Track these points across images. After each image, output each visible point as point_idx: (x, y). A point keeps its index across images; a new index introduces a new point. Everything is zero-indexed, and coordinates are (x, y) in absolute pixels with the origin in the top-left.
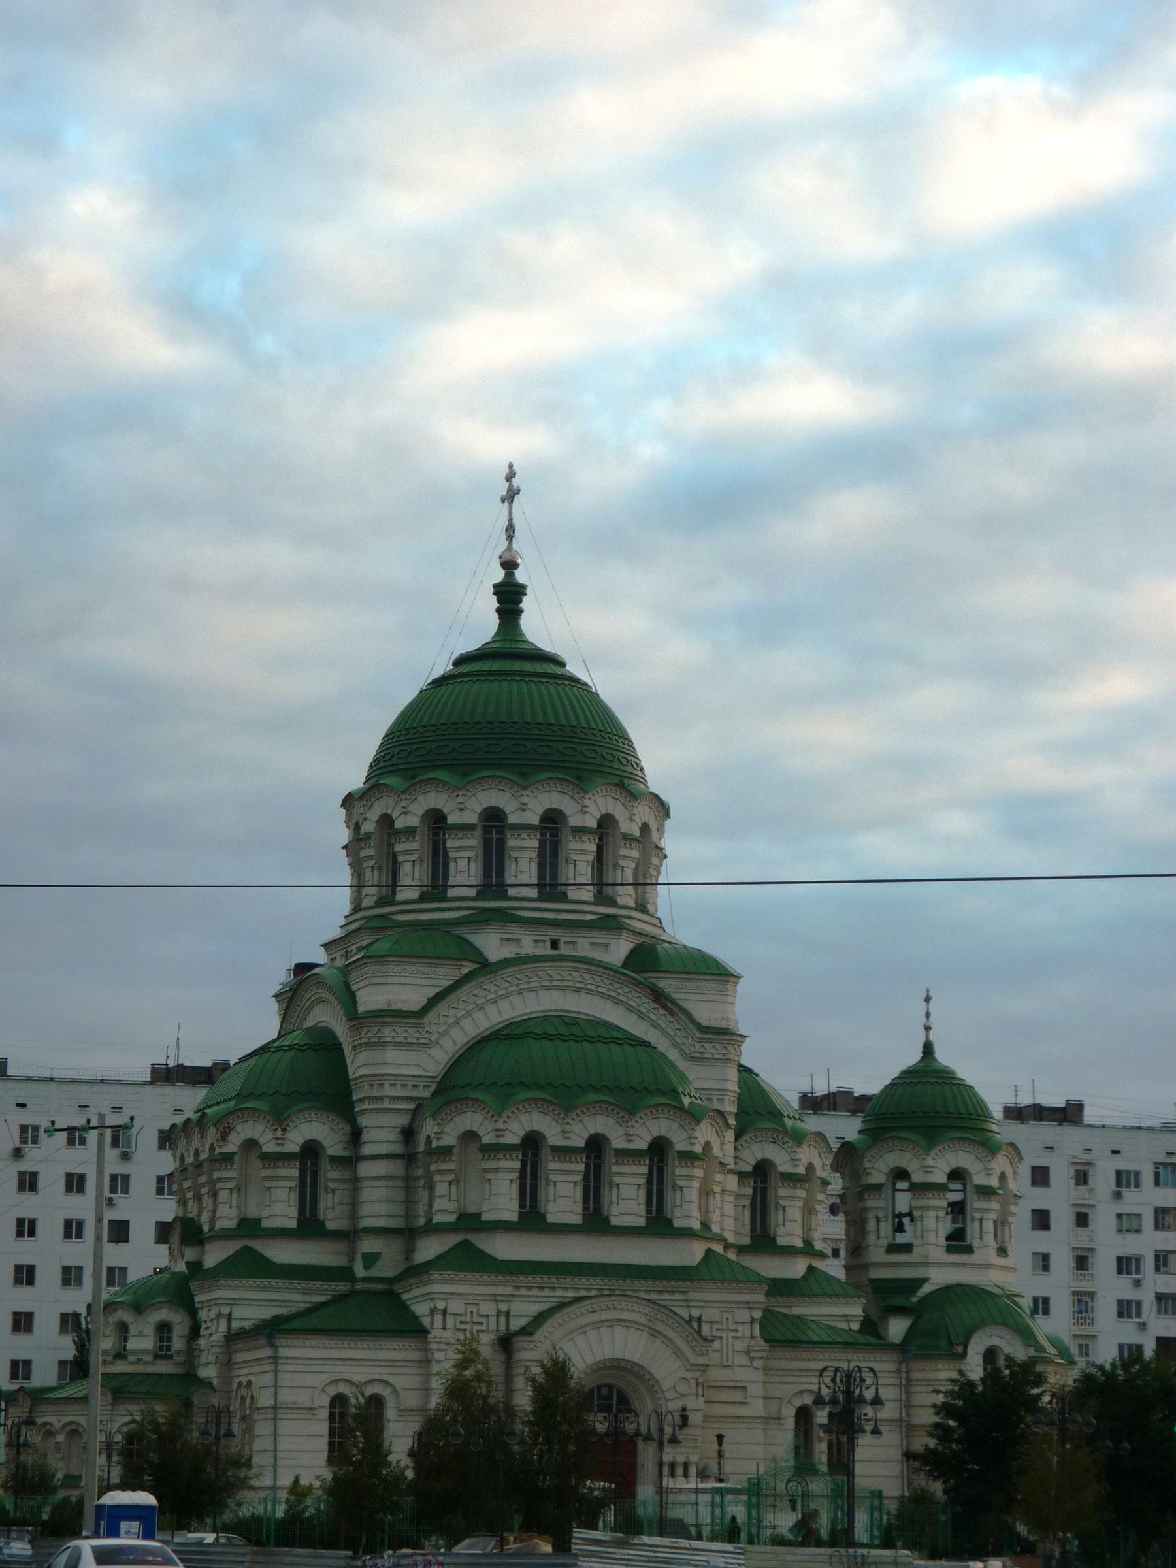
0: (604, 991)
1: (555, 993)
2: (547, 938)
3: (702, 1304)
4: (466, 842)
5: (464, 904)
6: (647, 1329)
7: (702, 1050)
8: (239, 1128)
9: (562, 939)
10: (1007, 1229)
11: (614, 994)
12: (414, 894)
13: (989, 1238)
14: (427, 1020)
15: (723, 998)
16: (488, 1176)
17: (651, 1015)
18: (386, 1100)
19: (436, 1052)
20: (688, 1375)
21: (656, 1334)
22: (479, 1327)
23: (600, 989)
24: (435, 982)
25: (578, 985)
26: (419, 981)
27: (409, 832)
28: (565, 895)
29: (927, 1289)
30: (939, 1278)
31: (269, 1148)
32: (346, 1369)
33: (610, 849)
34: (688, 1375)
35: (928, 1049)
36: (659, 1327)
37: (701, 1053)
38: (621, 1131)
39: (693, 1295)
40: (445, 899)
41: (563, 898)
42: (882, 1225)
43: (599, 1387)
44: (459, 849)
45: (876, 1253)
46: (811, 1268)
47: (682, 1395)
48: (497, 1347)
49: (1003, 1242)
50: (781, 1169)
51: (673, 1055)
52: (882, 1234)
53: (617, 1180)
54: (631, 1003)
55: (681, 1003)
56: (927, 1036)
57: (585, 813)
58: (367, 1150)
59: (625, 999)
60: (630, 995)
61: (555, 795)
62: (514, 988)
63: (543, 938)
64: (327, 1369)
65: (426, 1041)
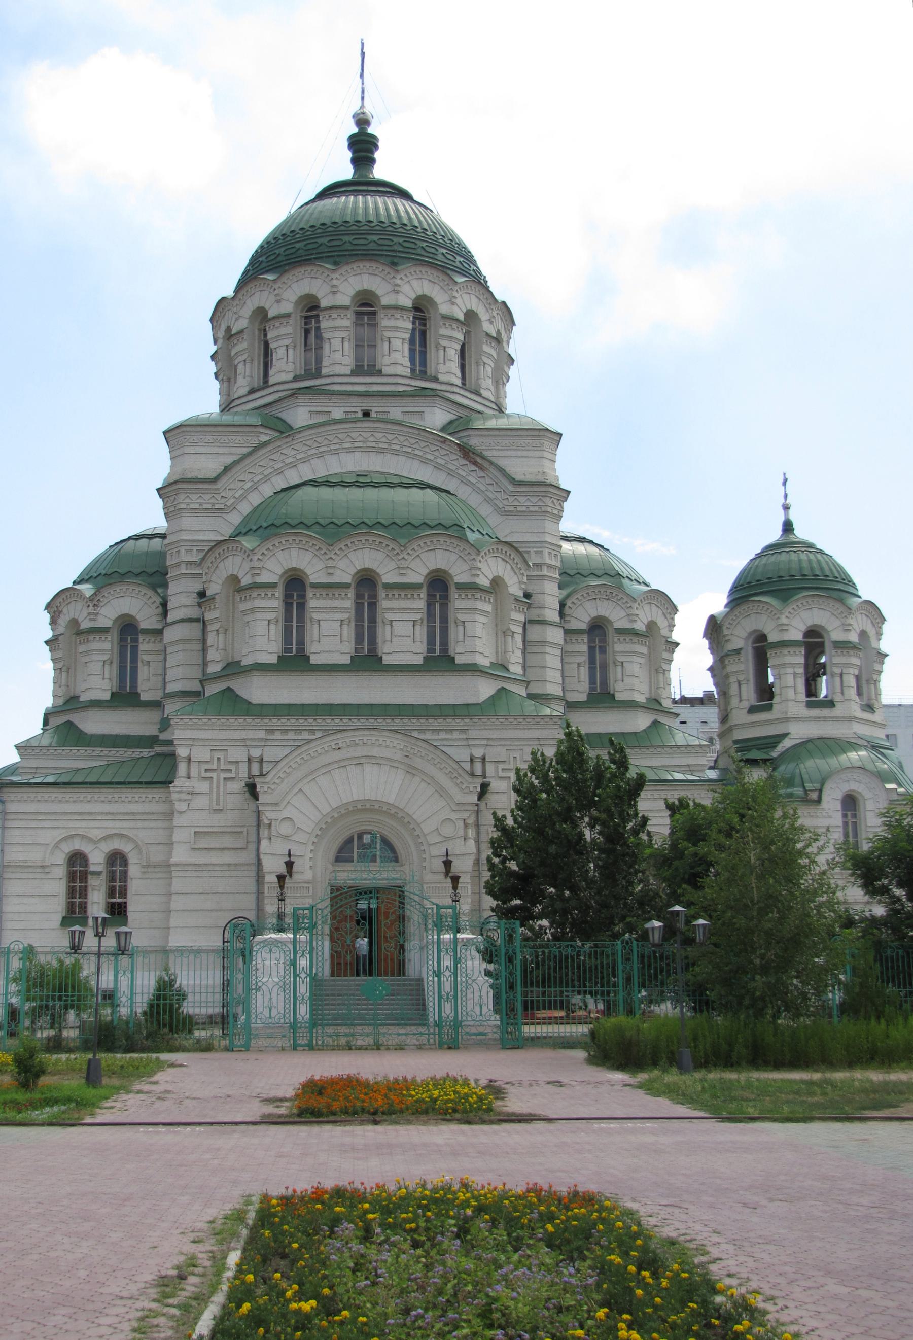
0: (409, 450)
1: (358, 455)
2: (359, 410)
3: (485, 742)
4: (283, 331)
5: (281, 387)
6: (403, 767)
7: (516, 503)
8: (65, 610)
9: (374, 410)
10: (873, 686)
11: (421, 453)
12: (244, 391)
13: (852, 692)
14: (219, 485)
15: (537, 453)
16: (247, 618)
17: (460, 472)
18: (183, 566)
19: (230, 517)
20: (454, 816)
21: (414, 772)
22: (228, 775)
23: (405, 449)
24: (233, 450)
25: (381, 445)
26: (216, 450)
27: (241, 332)
28: (380, 371)
29: (787, 743)
30: (798, 732)
31: (85, 625)
32: (84, 824)
33: (432, 331)
34: (454, 816)
35: (788, 527)
36: (418, 762)
37: (515, 506)
38: (392, 565)
39: (473, 733)
40: (268, 387)
41: (379, 373)
42: (744, 688)
43: (360, 836)
44: (278, 338)
45: (739, 716)
46: (655, 723)
47: (448, 839)
48: (247, 794)
49: (869, 699)
50: (617, 625)
51: (485, 510)
52: (744, 697)
53: (390, 616)
54: (439, 460)
55: (494, 460)
56: (786, 514)
57: (397, 292)
58: (170, 619)
59: (432, 458)
60: (436, 453)
61: (365, 277)
62: (313, 451)
63: (354, 409)
64: (61, 824)
65: (222, 506)
